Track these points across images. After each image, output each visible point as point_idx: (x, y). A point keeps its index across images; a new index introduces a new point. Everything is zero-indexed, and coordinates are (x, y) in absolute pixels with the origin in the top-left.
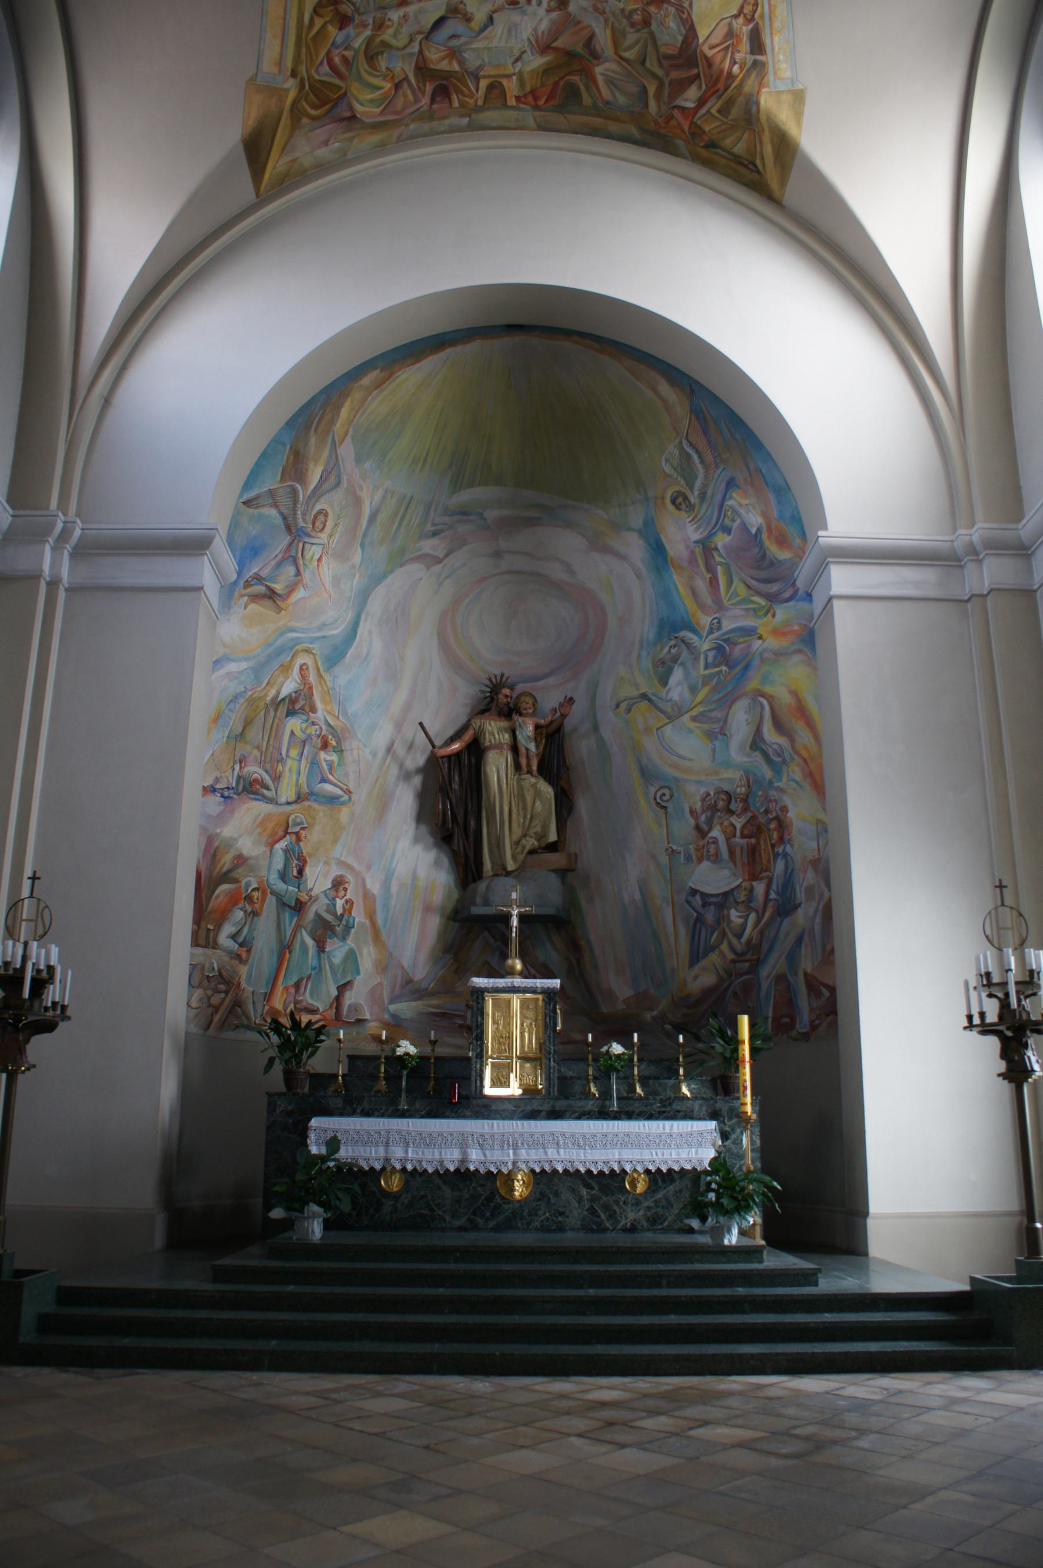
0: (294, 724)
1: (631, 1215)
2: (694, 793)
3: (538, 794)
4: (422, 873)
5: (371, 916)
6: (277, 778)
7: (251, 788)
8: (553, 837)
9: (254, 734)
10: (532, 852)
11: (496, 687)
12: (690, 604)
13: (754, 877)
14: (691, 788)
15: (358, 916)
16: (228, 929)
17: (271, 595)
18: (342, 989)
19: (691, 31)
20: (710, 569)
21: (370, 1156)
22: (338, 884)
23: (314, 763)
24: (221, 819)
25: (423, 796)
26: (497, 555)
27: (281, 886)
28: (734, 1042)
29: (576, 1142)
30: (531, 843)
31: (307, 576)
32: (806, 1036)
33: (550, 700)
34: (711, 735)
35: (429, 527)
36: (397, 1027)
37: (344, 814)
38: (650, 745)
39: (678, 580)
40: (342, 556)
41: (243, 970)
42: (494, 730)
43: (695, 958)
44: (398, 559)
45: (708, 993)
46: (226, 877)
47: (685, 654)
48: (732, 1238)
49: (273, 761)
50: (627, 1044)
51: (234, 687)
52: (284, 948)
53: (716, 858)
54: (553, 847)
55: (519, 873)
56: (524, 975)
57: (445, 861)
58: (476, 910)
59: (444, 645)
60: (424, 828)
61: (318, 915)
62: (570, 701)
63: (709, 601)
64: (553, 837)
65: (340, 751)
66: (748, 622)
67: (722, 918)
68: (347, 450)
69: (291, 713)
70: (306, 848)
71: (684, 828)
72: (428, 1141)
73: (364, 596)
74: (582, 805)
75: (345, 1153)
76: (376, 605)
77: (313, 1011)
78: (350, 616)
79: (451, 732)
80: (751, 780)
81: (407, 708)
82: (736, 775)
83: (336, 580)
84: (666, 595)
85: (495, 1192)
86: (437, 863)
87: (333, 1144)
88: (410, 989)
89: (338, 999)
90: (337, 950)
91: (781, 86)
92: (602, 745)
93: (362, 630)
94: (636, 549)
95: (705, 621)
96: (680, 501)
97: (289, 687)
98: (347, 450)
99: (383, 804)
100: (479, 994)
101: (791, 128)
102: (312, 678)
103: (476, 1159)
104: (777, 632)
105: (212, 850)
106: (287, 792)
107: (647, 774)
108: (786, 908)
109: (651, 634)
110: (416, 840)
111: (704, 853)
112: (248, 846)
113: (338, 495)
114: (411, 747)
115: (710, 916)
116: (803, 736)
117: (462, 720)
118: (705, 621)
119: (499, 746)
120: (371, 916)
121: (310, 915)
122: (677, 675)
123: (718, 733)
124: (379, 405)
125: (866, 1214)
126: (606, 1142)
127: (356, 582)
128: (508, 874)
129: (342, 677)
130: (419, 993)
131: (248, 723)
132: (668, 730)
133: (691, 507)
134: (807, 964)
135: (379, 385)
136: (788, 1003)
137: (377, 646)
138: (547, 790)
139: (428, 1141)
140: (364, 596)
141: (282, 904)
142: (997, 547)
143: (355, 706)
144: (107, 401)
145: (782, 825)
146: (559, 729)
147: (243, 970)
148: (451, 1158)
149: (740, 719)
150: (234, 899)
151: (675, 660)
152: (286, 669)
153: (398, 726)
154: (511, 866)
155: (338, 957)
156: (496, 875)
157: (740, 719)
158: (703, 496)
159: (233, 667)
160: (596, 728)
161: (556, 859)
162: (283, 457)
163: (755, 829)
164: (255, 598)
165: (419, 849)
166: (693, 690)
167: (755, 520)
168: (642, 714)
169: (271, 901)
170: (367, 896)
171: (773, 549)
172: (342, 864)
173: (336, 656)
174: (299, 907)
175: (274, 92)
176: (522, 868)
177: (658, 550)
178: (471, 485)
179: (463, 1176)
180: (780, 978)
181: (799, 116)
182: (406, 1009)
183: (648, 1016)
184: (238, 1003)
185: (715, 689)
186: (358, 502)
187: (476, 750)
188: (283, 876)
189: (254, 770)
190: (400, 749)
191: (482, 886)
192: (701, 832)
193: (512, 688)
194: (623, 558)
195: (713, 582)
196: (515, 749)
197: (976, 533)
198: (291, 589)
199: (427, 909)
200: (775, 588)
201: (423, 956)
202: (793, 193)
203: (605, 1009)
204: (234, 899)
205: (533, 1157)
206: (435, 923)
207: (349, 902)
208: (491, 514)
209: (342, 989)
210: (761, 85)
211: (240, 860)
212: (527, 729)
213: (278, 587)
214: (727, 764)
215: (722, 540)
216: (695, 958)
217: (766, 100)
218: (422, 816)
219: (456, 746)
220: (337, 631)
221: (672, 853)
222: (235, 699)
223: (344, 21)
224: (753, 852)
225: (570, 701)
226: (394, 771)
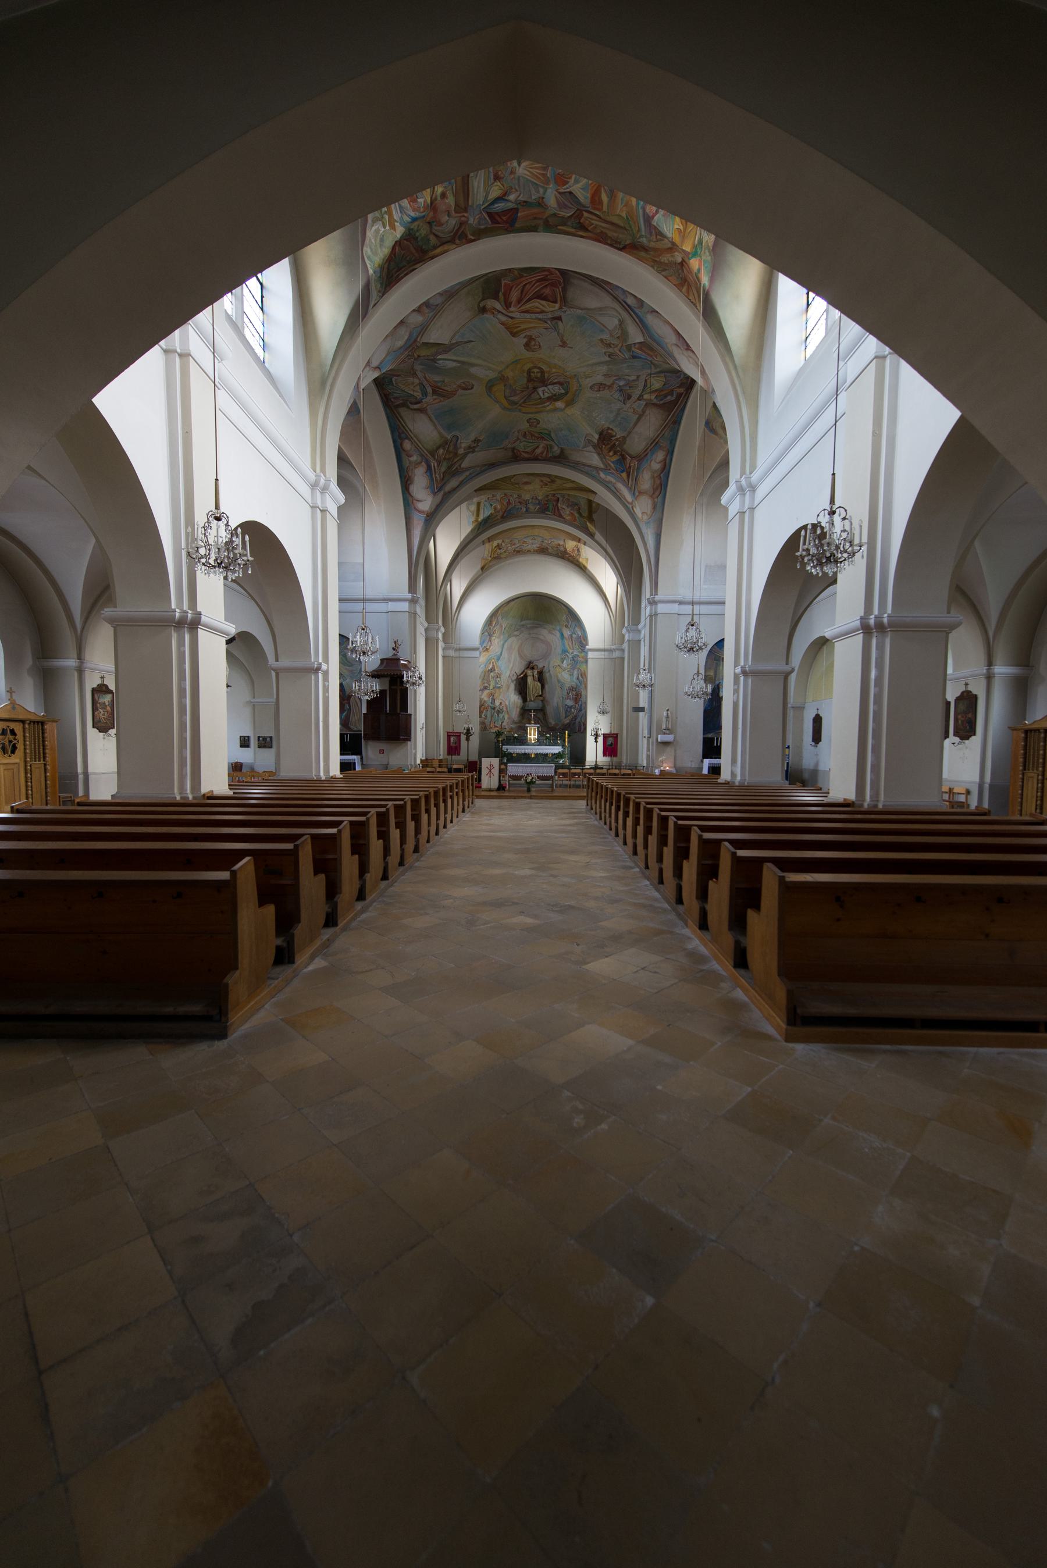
0: (492, 674)
1: (549, 760)
2: (567, 686)
3: (537, 685)
4: (516, 700)
5: (507, 709)
6: (489, 685)
7: (485, 688)
8: (540, 694)
9: (486, 678)
10: (537, 696)
11: (530, 663)
12: (567, 647)
13: (576, 703)
14: (567, 685)
15: (504, 709)
16: (483, 714)
17: (487, 649)
18: (502, 723)
19: (566, 550)
20: (572, 641)
21: (512, 751)
22: (501, 703)
23: (496, 680)
24: (481, 695)
25: (515, 685)
26: (530, 634)
27: (491, 705)
28: (565, 734)
29: (541, 749)
30: (536, 695)
31: (493, 643)
32: (582, 733)
33: (540, 666)
34: (570, 675)
35: (516, 629)
36: (512, 729)
37: (501, 690)
38: (559, 676)
39: (566, 642)
40: (499, 638)
41: (486, 721)
42: (529, 672)
43: (566, 718)
44: (509, 637)
45: (568, 724)
46: (483, 705)
47: (567, 658)
48: (561, 762)
49: (489, 682)
50: (550, 734)
51: (482, 670)
52: (492, 716)
53: (570, 699)
54: (541, 696)
55: (534, 701)
56: (534, 724)
57: (520, 698)
58: (527, 708)
59: (519, 654)
60: (516, 692)
61: (498, 710)
62: (544, 667)
63: (571, 647)
64: (540, 694)
65: (500, 678)
66: (577, 654)
67: (571, 711)
68: (500, 618)
69: (491, 672)
70: (495, 698)
71: (565, 692)
72: (520, 749)
73: (503, 645)
74: (546, 686)
75: (509, 751)
76: (506, 646)
77: (497, 727)
78: (501, 650)
79: (520, 672)
80: (577, 685)
81: (512, 668)
82: (574, 683)
83: (498, 643)
84: (564, 644)
85: (529, 756)
86: (518, 698)
87: (507, 750)
88: (514, 722)
89: (502, 724)
90: (501, 716)
91: (584, 557)
92: (550, 675)
93: (503, 652)
94: (558, 634)
95: (571, 651)
96: (566, 626)
97: (491, 667)
98: (500, 618)
99: (508, 687)
100: (527, 727)
101: (586, 565)
102: (494, 664)
103: (527, 752)
104: (583, 657)
105: (481, 701)
106: (491, 687)
107: (559, 681)
108: (581, 710)
109: (561, 652)
110: (515, 694)
111: (568, 698)
112: (486, 699)
113: (498, 626)
114: (513, 676)
115: (569, 709)
116: (585, 680)
117: (523, 669)
118: (571, 651)
119: (530, 676)
120: (507, 709)
121: (496, 709)
122: (565, 662)
123: (572, 675)
124: (506, 609)
125: (585, 760)
126: (546, 749)
127: (502, 642)
128: (532, 701)
129: (500, 662)
130: (516, 723)
131: (484, 676)
132: (563, 673)
133: (568, 628)
134: (583, 720)
135: (506, 606)
136: (580, 726)
137: (506, 655)
138: (539, 684)
139: (520, 749)
140: (503, 645)
141: (491, 708)
142: (618, 649)
143: (502, 669)
144: (457, 618)
145: (581, 695)
146: (542, 672)
147: (486, 721)
148: (523, 752)
149: (576, 672)
150: (484, 709)
151: (565, 658)
152: (490, 663)
153: (511, 671)
154: (532, 699)
155: (501, 717)
156: (530, 701)
157: (576, 672)
158: (570, 626)
159: (482, 666)
160: (549, 671)
161: (541, 698)
162: (489, 622)
163: (577, 695)
164: (484, 651)
165: (515, 696)
166: (568, 665)
167: (580, 634)
168: (558, 669)
169: (489, 709)
170: (506, 706)
171: (583, 641)
172: (501, 699)
173: (498, 659)
174: (494, 708)
175: (487, 559)
176: (535, 700)
177: (562, 635)
178: (525, 620)
179: (525, 754)
180: (579, 722)
181: (587, 563)
182: (513, 726)
183: (557, 727)
184: (485, 726)
185: (572, 665)
186: (502, 626)
187: (526, 676)
188: (491, 703)
189: (486, 685)
190: (511, 676)
191: (527, 703)
192: (568, 694)
193: (533, 663)
194: (555, 636)
195: (572, 644)
196: (533, 676)
197: (614, 647)
198: (490, 647)
199: (517, 707)
200: (582, 648)
201: (516, 716)
202: (587, 571)
203: (550, 726)
204: (484, 709)
205: (535, 751)
206: (518, 710)
207: (503, 707)
208: (528, 626)
209: (502, 723)
210: (579, 557)
211: (485, 701)
212: (536, 673)
213: (488, 647)
214: (574, 682)
215: (574, 636)
216: (566, 718)
217: (580, 560)
218: (515, 690)
219: (522, 675)
220: (499, 653)
221: (563, 697)
222: (482, 672)
223: (500, 549)
224: (576, 699)
225: (544, 667)
226: (510, 680)
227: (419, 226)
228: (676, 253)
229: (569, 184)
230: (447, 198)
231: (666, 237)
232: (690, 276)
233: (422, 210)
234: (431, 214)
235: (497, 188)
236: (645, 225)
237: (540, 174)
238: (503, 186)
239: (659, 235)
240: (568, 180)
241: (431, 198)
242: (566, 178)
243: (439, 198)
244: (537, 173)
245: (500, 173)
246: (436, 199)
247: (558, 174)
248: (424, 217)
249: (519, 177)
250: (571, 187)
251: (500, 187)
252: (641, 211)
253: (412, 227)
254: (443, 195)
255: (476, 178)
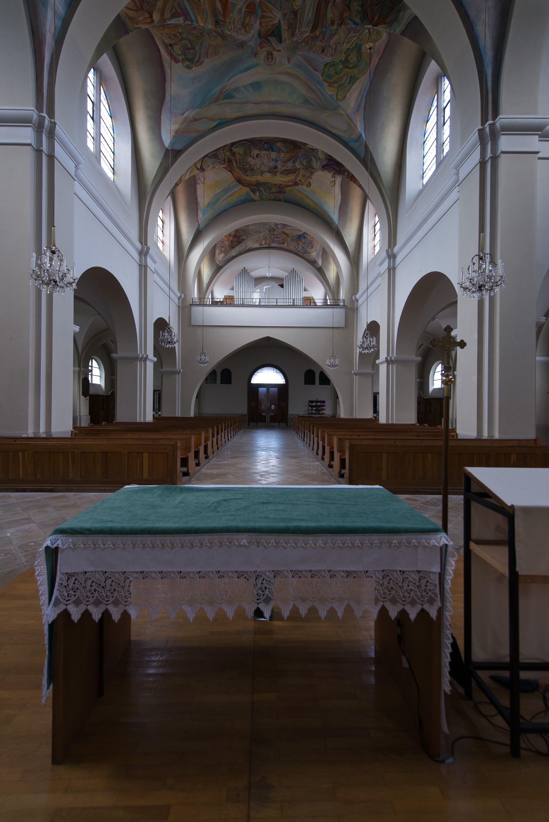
227: (356, 15)
228: (158, 18)
229: (245, 6)
230: (331, 18)
231: (170, 19)
232: (141, 18)
233: (349, 26)
234: (346, 14)
235: (297, 4)
236: (186, 9)
237: (266, 12)
238: (292, 3)
239: (175, 12)
240: (246, 10)
241: (341, 27)
242: (249, 11)
243: (336, 23)
244: (268, 13)
245: (293, 17)
246: (338, 25)
247: (253, 14)
248: (350, 19)
249: (280, 10)
250: (244, 4)
251: (295, 4)
252: (193, 18)
253: (360, 21)
254: (333, 23)
255: (309, 21)
